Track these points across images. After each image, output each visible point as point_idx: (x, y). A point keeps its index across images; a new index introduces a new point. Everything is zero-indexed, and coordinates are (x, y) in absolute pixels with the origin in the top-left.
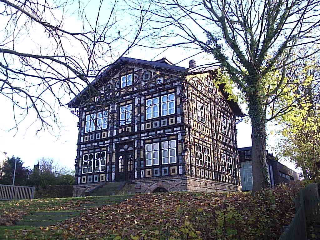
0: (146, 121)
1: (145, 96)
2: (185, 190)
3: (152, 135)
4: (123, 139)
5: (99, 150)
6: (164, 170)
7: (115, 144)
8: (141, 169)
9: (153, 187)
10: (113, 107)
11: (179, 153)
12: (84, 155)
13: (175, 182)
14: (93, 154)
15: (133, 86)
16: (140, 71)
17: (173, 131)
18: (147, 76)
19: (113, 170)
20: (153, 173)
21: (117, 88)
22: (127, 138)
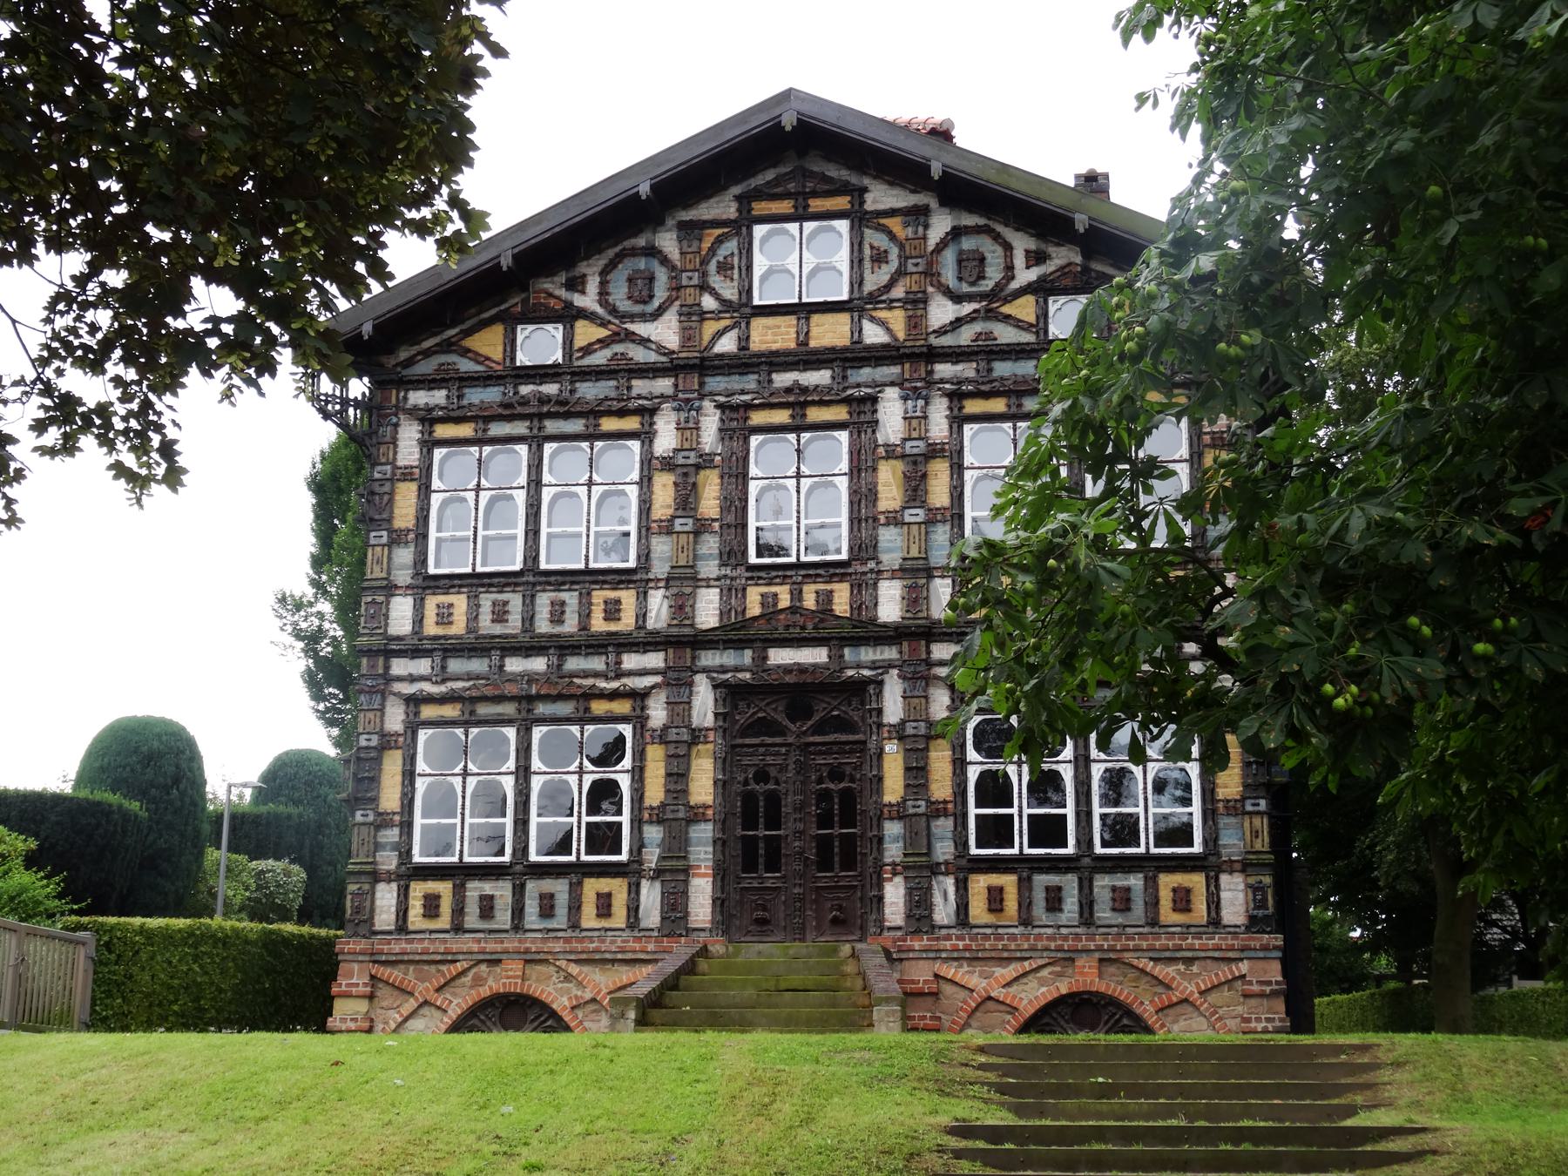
1: (956, 397)
2: (1268, 1020)
4: (780, 657)
6: (1114, 889)
8: (934, 869)
9: (1034, 994)
10: (690, 429)
12: (423, 735)
13: (1195, 969)
15: (857, 306)
16: (922, 219)
18: (972, 265)
20: (1025, 905)
21: (717, 296)
22: (816, 656)
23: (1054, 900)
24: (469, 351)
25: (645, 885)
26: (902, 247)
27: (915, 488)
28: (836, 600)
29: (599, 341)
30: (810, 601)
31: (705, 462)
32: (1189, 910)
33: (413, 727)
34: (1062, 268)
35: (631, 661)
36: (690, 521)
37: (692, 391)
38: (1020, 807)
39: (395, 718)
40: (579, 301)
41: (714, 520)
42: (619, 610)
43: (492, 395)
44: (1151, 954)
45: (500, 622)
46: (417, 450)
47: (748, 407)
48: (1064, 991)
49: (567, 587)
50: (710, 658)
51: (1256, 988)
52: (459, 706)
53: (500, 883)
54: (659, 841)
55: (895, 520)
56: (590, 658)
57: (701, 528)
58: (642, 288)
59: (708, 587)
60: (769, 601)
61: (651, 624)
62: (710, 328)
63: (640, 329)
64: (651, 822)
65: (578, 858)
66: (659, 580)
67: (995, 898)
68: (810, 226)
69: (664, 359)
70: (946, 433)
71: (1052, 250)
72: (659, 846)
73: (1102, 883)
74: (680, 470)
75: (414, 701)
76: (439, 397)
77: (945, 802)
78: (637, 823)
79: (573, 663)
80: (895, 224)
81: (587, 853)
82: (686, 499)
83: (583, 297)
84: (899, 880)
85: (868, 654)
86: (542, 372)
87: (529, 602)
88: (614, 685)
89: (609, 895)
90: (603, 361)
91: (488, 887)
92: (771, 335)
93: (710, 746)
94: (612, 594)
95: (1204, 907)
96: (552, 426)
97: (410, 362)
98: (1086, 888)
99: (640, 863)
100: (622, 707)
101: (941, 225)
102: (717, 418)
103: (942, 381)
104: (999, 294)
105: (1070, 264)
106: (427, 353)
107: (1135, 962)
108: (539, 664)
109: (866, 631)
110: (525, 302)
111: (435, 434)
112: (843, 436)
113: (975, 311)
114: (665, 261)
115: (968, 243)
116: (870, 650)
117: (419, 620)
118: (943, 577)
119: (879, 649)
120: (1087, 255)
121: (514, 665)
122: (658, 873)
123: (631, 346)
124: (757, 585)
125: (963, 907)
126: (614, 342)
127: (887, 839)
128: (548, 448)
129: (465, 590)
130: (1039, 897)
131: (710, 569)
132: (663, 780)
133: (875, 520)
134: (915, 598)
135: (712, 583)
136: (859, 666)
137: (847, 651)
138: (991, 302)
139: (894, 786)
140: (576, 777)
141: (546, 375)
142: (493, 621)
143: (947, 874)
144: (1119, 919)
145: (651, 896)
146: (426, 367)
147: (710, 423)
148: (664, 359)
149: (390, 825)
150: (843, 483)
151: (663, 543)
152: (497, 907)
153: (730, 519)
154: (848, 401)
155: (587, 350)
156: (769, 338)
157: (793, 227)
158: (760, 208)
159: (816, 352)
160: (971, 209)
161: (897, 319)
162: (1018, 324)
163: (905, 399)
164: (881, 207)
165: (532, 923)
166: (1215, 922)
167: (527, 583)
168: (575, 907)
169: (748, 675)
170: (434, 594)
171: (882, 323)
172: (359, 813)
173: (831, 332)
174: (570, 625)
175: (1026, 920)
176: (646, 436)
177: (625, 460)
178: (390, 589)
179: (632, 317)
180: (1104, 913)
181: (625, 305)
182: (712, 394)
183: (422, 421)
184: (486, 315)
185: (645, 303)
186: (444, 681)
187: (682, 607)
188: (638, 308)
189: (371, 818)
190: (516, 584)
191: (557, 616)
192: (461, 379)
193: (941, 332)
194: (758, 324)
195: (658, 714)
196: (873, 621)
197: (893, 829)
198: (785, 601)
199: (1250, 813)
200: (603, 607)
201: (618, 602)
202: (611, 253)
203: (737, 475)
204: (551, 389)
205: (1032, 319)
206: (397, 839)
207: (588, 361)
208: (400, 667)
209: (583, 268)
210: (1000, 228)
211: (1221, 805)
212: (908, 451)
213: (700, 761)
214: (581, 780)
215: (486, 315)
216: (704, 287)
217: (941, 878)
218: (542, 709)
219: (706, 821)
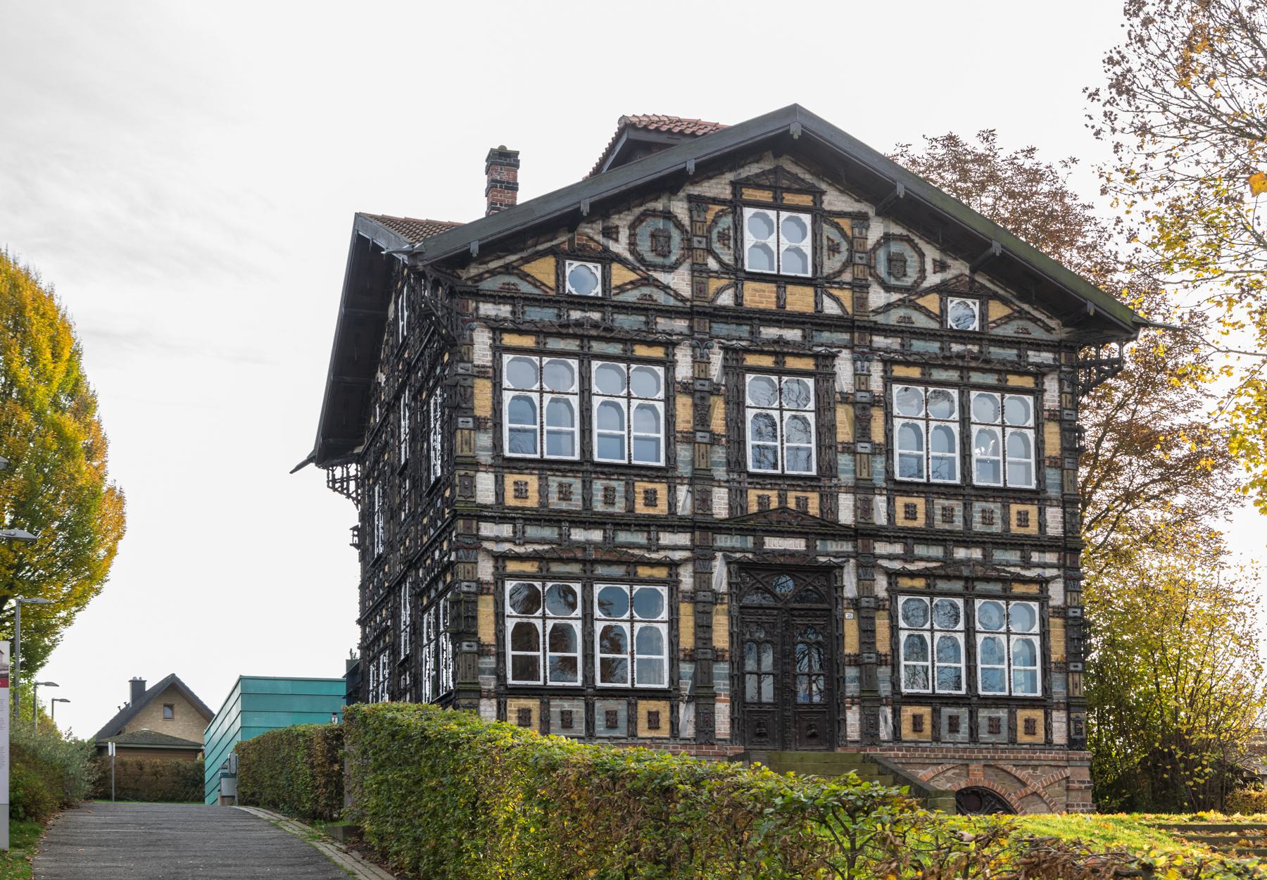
0: (897, 488)
1: (888, 363)
2: (1084, 806)
3: (929, 559)
4: (773, 543)
5: (618, 571)
6: (990, 719)
7: (729, 562)
8: (880, 701)
10: (700, 362)
11: (1054, 658)
13: (1038, 772)
14: (577, 587)
15: (819, 283)
17: (1027, 564)
18: (897, 264)
19: (722, 686)
20: (935, 726)
22: (798, 545)
23: (954, 725)
24: (528, 275)
25: (682, 706)
26: (851, 243)
27: (862, 427)
28: (810, 505)
29: (631, 283)
30: (792, 504)
31: (715, 391)
32: (1034, 734)
33: (501, 577)
34: (956, 277)
35: (666, 538)
36: (708, 435)
37: (705, 333)
38: (933, 661)
39: (485, 570)
40: (616, 248)
41: (723, 436)
42: (656, 499)
43: (546, 315)
44: (1014, 763)
45: (564, 499)
46: (490, 353)
47: (747, 351)
48: (963, 787)
49: (616, 477)
50: (723, 541)
51: (1076, 785)
52: (536, 564)
53: (576, 702)
54: (691, 675)
55: (849, 449)
56: (635, 534)
57: (714, 440)
58: (660, 242)
59: (720, 486)
60: (762, 501)
61: (680, 512)
62: (714, 284)
63: (663, 277)
64: (684, 661)
65: (633, 684)
66: (681, 478)
67: (917, 722)
68: (784, 215)
69: (680, 304)
70: (881, 389)
71: (950, 261)
72: (691, 679)
73: (983, 714)
74: (697, 395)
75: (500, 558)
76: (505, 310)
77: (886, 655)
78: (674, 661)
79: (623, 537)
80: (845, 223)
82: (702, 418)
83: (616, 245)
84: (855, 708)
85: (833, 546)
86: (592, 302)
87: (587, 486)
88: (654, 556)
89: (657, 713)
90: (634, 299)
91: (567, 705)
92: (759, 297)
93: (725, 607)
94: (650, 486)
95: (1043, 732)
96: (597, 347)
97: (480, 277)
98: (973, 716)
99: (678, 689)
100: (661, 573)
101: (876, 231)
102: (721, 356)
103: (879, 349)
104: (915, 290)
105: (962, 275)
106: (493, 273)
107: (1005, 767)
108: (597, 535)
109: (827, 528)
110: (571, 241)
111: (503, 342)
112: (810, 382)
113: (900, 300)
114: (679, 225)
115: (895, 248)
116: (834, 544)
117: (500, 493)
118: (881, 494)
119: (840, 543)
120: (973, 271)
121: (578, 535)
122: (691, 699)
123: (655, 290)
124: (755, 488)
125: (897, 729)
126: (643, 285)
127: (847, 680)
128: (595, 364)
129: (536, 472)
130: (945, 722)
131: (720, 473)
132: (692, 630)
133: (836, 448)
134: (864, 509)
135: (722, 484)
136: (827, 555)
137: (818, 543)
138: (910, 295)
139: (851, 644)
140: (628, 624)
141: (594, 305)
142: (560, 499)
143: (886, 705)
144: (993, 739)
145: (686, 714)
146: (489, 285)
147: (717, 358)
148: (680, 304)
149: (488, 654)
150: (811, 418)
151: (685, 450)
152: (574, 720)
153: (734, 436)
154: (816, 356)
155: (622, 289)
156: (757, 299)
157: (772, 214)
158: (749, 194)
159: (792, 314)
160: (898, 220)
161: (846, 296)
162: (928, 313)
163: (854, 361)
164: (835, 209)
165: (601, 732)
166: (1049, 742)
167: (587, 471)
168: (632, 720)
169: (750, 556)
170: (511, 473)
171: (836, 299)
172: (465, 644)
173: (800, 301)
174: (619, 507)
175: (936, 738)
176: (669, 364)
177: (649, 382)
178: (476, 465)
179: (655, 267)
180: (984, 735)
181: (650, 257)
182: (717, 337)
183: (493, 330)
184: (540, 248)
185: (664, 256)
186: (523, 545)
188: (659, 260)
189: (475, 649)
190: (578, 471)
191: (609, 498)
192: (526, 299)
193: (876, 312)
194: (749, 286)
195: (687, 580)
196: (835, 523)
197: (851, 672)
198: (774, 504)
199: (1072, 672)
200: (643, 495)
201: (655, 492)
202: (637, 211)
203: (736, 403)
204: (596, 316)
205: (937, 311)
206: (494, 666)
207: (621, 298)
208: (487, 529)
209: (615, 220)
210: (917, 240)
211: (1053, 665)
212: (858, 399)
213: (718, 617)
214: (632, 627)
215: (540, 248)
216: (710, 251)
217: (882, 708)
218: (600, 570)
219: (723, 661)
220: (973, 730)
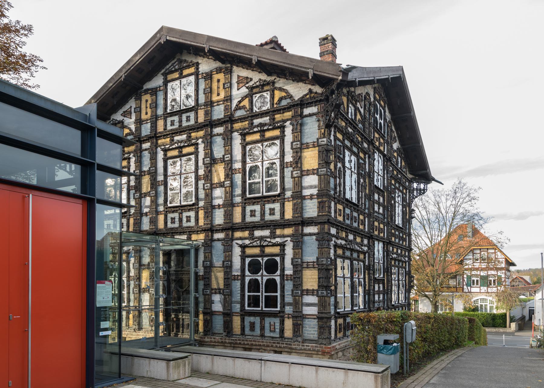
81: (265, 307)
100: (276, 250)
187: (299, 209)
214: (262, 279)
220: (262, 328)
